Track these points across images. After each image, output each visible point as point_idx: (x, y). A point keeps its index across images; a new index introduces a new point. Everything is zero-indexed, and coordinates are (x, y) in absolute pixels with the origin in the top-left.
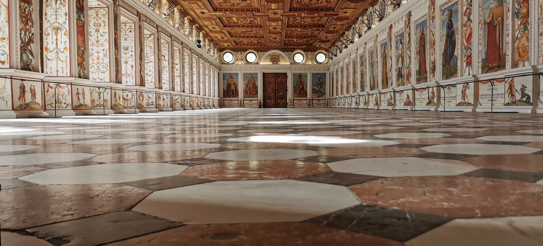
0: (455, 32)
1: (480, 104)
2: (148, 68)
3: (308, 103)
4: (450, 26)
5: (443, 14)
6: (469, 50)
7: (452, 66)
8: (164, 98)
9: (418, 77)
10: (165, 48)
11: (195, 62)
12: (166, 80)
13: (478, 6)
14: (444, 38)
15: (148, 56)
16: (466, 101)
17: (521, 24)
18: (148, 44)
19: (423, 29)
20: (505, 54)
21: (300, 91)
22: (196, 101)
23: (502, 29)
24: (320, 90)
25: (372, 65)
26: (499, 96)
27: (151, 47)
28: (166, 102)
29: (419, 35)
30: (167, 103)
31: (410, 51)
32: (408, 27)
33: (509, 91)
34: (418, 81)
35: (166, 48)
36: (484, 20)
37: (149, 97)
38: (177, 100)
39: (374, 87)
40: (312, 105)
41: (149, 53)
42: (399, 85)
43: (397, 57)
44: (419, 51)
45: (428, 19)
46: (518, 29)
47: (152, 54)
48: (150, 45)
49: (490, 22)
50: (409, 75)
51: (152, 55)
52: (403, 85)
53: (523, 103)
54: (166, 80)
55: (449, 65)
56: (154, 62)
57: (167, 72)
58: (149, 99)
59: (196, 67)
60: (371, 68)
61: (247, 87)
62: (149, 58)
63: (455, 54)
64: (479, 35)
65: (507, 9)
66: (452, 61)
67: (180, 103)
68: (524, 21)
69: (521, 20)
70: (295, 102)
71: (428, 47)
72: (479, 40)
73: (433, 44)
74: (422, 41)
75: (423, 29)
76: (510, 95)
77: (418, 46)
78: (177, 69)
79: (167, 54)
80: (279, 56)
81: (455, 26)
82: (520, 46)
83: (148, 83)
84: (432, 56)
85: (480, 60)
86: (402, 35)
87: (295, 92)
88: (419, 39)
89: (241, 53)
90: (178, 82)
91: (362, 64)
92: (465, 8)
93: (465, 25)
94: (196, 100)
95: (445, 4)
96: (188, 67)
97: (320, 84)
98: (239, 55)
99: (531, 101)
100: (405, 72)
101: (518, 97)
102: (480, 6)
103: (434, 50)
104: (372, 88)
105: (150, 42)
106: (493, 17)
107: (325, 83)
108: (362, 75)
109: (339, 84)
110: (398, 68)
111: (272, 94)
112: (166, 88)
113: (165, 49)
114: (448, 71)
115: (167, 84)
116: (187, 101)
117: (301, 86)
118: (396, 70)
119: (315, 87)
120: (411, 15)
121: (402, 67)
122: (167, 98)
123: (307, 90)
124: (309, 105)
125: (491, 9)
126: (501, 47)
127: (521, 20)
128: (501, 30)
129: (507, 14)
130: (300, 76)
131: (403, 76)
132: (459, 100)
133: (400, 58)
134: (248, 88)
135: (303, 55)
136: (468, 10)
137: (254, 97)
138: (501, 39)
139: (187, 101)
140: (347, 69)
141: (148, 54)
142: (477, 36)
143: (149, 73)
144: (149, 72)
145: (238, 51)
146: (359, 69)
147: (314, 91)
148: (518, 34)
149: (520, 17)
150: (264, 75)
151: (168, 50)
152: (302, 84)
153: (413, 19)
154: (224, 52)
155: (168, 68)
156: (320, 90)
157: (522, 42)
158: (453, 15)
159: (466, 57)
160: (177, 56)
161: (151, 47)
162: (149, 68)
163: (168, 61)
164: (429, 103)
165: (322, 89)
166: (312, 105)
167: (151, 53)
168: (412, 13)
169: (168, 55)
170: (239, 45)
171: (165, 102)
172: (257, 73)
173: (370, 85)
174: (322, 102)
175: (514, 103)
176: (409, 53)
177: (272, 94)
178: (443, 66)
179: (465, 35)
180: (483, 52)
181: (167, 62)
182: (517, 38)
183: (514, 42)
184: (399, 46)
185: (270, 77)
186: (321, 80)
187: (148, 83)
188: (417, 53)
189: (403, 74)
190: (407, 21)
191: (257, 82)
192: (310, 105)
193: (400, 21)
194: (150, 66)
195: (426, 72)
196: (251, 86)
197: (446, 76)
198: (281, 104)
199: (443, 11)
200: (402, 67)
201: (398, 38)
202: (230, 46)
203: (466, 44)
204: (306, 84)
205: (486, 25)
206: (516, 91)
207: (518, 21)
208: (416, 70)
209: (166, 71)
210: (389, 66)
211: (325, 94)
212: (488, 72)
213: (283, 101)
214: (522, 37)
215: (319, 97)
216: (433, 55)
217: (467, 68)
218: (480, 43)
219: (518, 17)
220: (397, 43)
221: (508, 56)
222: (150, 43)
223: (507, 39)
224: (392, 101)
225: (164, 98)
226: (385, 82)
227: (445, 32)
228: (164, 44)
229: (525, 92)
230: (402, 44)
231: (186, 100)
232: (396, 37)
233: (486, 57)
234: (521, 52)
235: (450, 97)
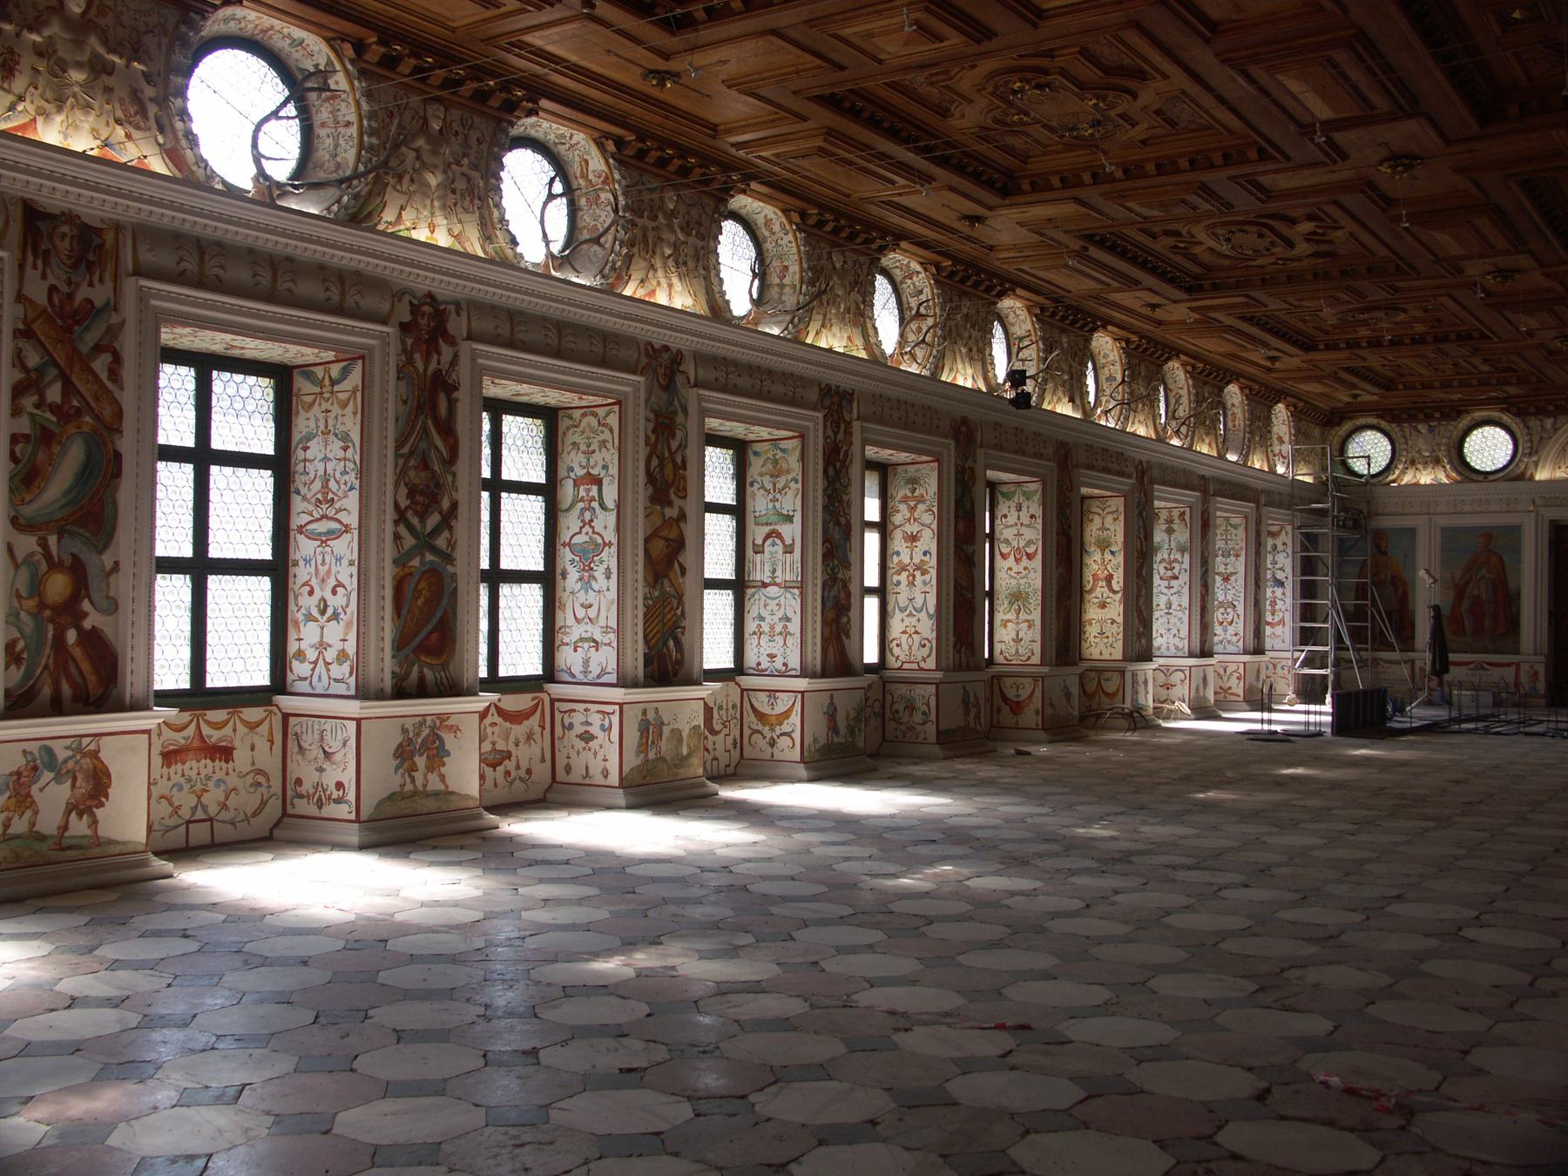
2: (329, 571)
8: (589, 728)
10: (607, 435)
11: (1036, 491)
12: (602, 622)
15: (330, 496)
18: (336, 418)
22: (1034, 700)
27: (345, 438)
28: (600, 756)
30: (605, 760)
35: (611, 430)
37: (325, 752)
38: (781, 724)
41: (338, 475)
47: (352, 478)
48: (342, 428)
51: (352, 488)
54: (602, 622)
56: (356, 533)
57: (608, 578)
58: (326, 765)
59: (1040, 521)
61: (1460, 593)
62: (337, 506)
67: (797, 736)
78: (788, 542)
79: (614, 470)
83: (327, 664)
89: (1431, 430)
90: (788, 620)
94: (1038, 694)
96: (934, 526)
98: (1421, 442)
105: (344, 405)
112: (603, 673)
113: (601, 437)
115: (609, 644)
116: (924, 713)
122: (602, 728)
134: (1466, 604)
137: (1497, 651)
139: (925, 708)
141: (332, 485)
143: (331, 600)
144: (334, 592)
145: (1419, 421)
151: (617, 444)
154: (1348, 426)
155: (614, 549)
160: (788, 472)
161: (345, 438)
162: (334, 569)
163: (618, 507)
167: (345, 472)
169: (616, 476)
170: (1401, 387)
171: (595, 754)
172: (1514, 532)
181: (611, 519)
187: (327, 664)
194: (339, 560)
202: (1359, 399)
209: (602, 569)
222: (345, 412)
225: (589, 728)
228: (601, 412)
231: (919, 703)
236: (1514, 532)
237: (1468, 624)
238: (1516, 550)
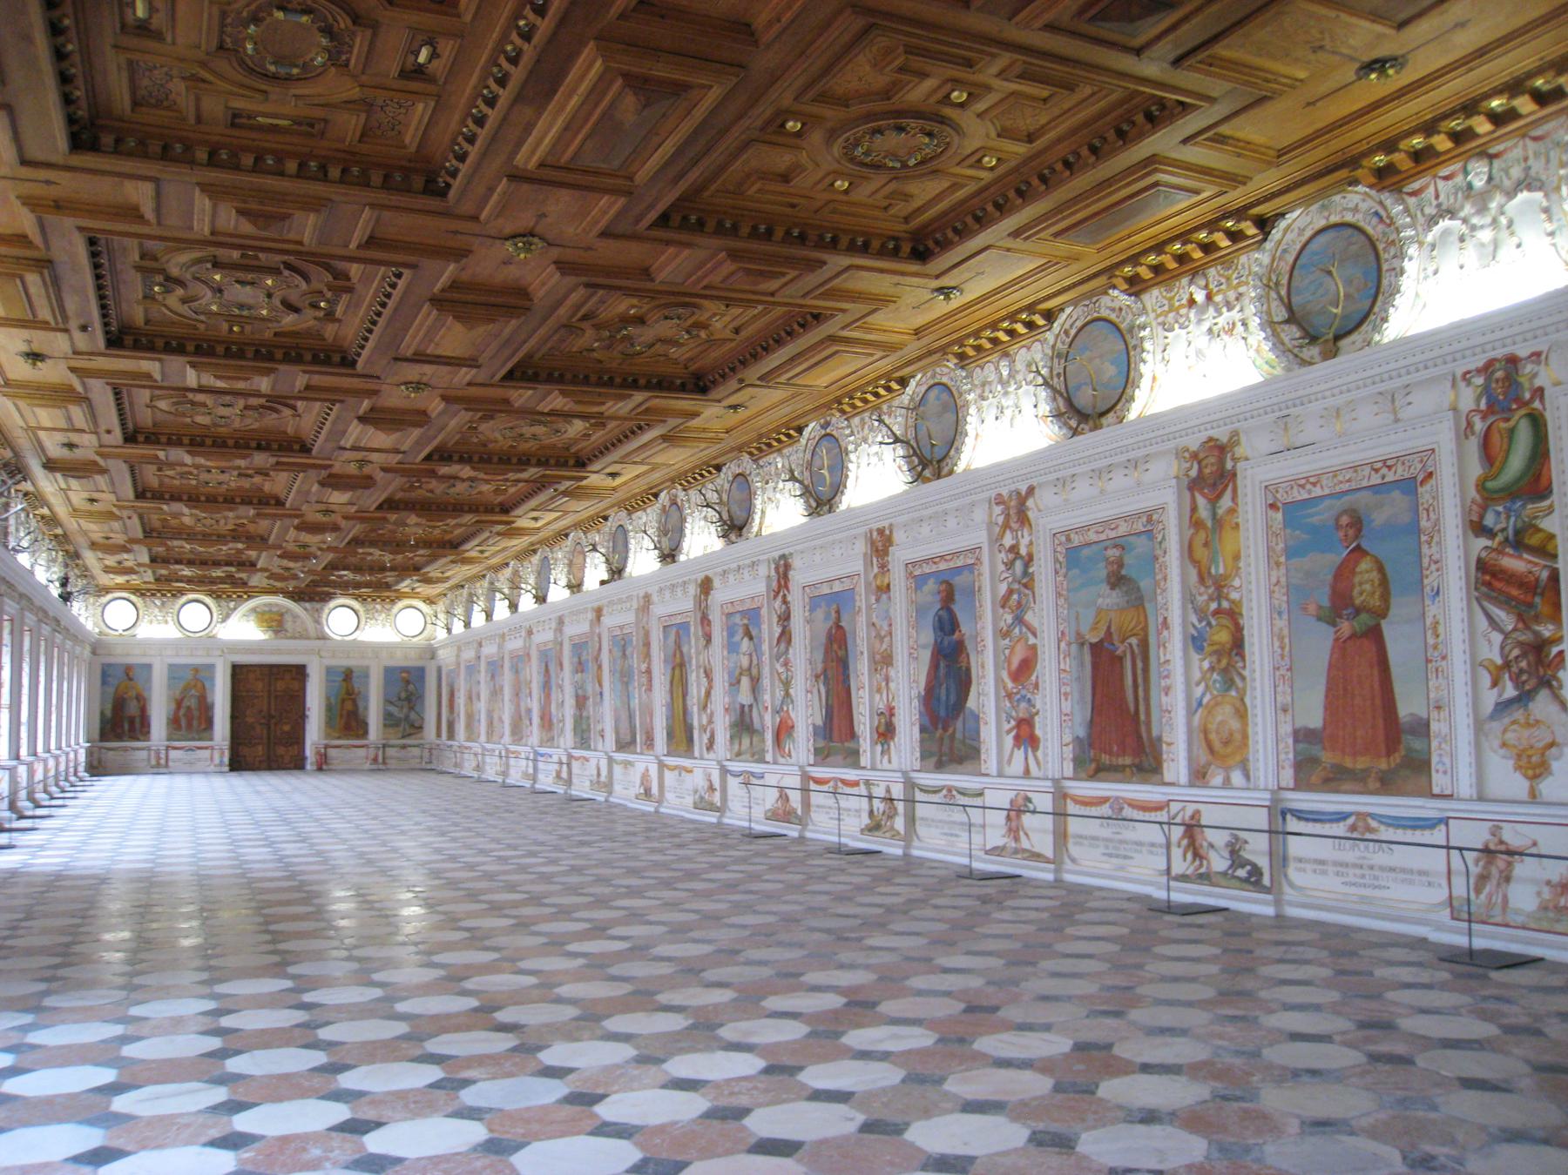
0: (969, 645)
1: (1073, 860)
3: (372, 756)
4: (947, 624)
5: (918, 588)
6: (1023, 705)
7: (959, 735)
9: (821, 744)
13: (1052, 596)
14: (926, 656)
16: (1025, 844)
17: (1212, 669)
19: (838, 612)
20: (1160, 739)
21: (347, 719)
23: (1146, 670)
24: (407, 717)
25: (623, 674)
26: (1144, 849)
29: (823, 626)
31: (786, 664)
32: (780, 598)
33: (1185, 842)
34: (822, 755)
36: (1079, 634)
39: (633, 741)
40: (384, 763)
42: (739, 754)
43: (730, 674)
44: (825, 671)
45: (861, 589)
46: (1203, 678)
49: (1101, 641)
50: (783, 731)
53: (1234, 882)
55: (945, 729)
60: (619, 686)
63: (971, 703)
64: (1061, 671)
65: (1160, 620)
66: (959, 724)
68: (1224, 662)
69: (1214, 659)
70: (332, 753)
71: (861, 669)
72: (1061, 683)
73: (887, 660)
74: (835, 646)
75: (838, 612)
76: (1189, 856)
77: (819, 656)
80: (282, 615)
81: (965, 628)
82: (1212, 727)
84: (877, 697)
85: (1068, 738)
86: (753, 615)
87: (330, 722)
88: (823, 639)
91: (580, 667)
92: (1003, 588)
93: (1006, 634)
95: (926, 561)
97: (408, 699)
99: (1266, 881)
100: (768, 721)
101: (1219, 863)
102: (1058, 595)
103: (887, 680)
104: (624, 745)
106: (1109, 633)
107: (421, 697)
108: (581, 701)
109: (482, 706)
111: (258, 728)
114: (945, 749)
117: (348, 705)
118: (726, 710)
119: (392, 709)
120: (787, 567)
121: (751, 706)
123: (366, 716)
124: (375, 760)
125: (1099, 611)
126: (1142, 717)
127: (1214, 659)
128: (1139, 672)
129: (1159, 633)
130: (348, 675)
132: (996, 837)
133: (745, 681)
135: (356, 612)
136: (1015, 596)
138: (1141, 693)
140: (516, 671)
142: (1055, 674)
146: (567, 678)
147: (390, 721)
148: (1203, 695)
149: (1208, 649)
150: (238, 671)
152: (354, 702)
153: (798, 578)
156: (407, 717)
157: (1219, 718)
158: (957, 597)
159: (1013, 723)
164: (874, 827)
165: (413, 716)
166: (384, 763)
168: (796, 562)
173: (617, 733)
174: (416, 751)
175: (1205, 878)
176: (781, 670)
177: (258, 728)
178: (923, 730)
179: (1008, 660)
180: (1078, 719)
182: (1200, 704)
183: (1190, 713)
184: (738, 644)
185: (251, 676)
186: (411, 687)
188: (817, 677)
189: (757, 724)
190: (775, 578)
191: (213, 691)
192: (380, 765)
193: (746, 575)
195: (852, 735)
196: (193, 703)
197: (934, 759)
198: (287, 759)
199: (919, 581)
200: (751, 706)
201: (737, 619)
203: (1010, 685)
204: (366, 699)
205: (1086, 649)
206: (1211, 846)
207: (1202, 660)
210: (695, 691)
211: (421, 728)
212: (1100, 775)
213: (294, 750)
214: (1217, 704)
215: (403, 737)
216: (879, 690)
217: (1019, 755)
218: (1066, 694)
219: (1199, 649)
220: (731, 632)
221: (1169, 744)
223: (1164, 699)
224: (717, 798)
226: (680, 733)
227: (928, 636)
229: (1242, 853)
230: (751, 638)
232: (729, 615)
233: (1090, 736)
234: (1217, 745)
235: (954, 823)
236: (211, 667)
237: (183, 722)
238: (212, 679)
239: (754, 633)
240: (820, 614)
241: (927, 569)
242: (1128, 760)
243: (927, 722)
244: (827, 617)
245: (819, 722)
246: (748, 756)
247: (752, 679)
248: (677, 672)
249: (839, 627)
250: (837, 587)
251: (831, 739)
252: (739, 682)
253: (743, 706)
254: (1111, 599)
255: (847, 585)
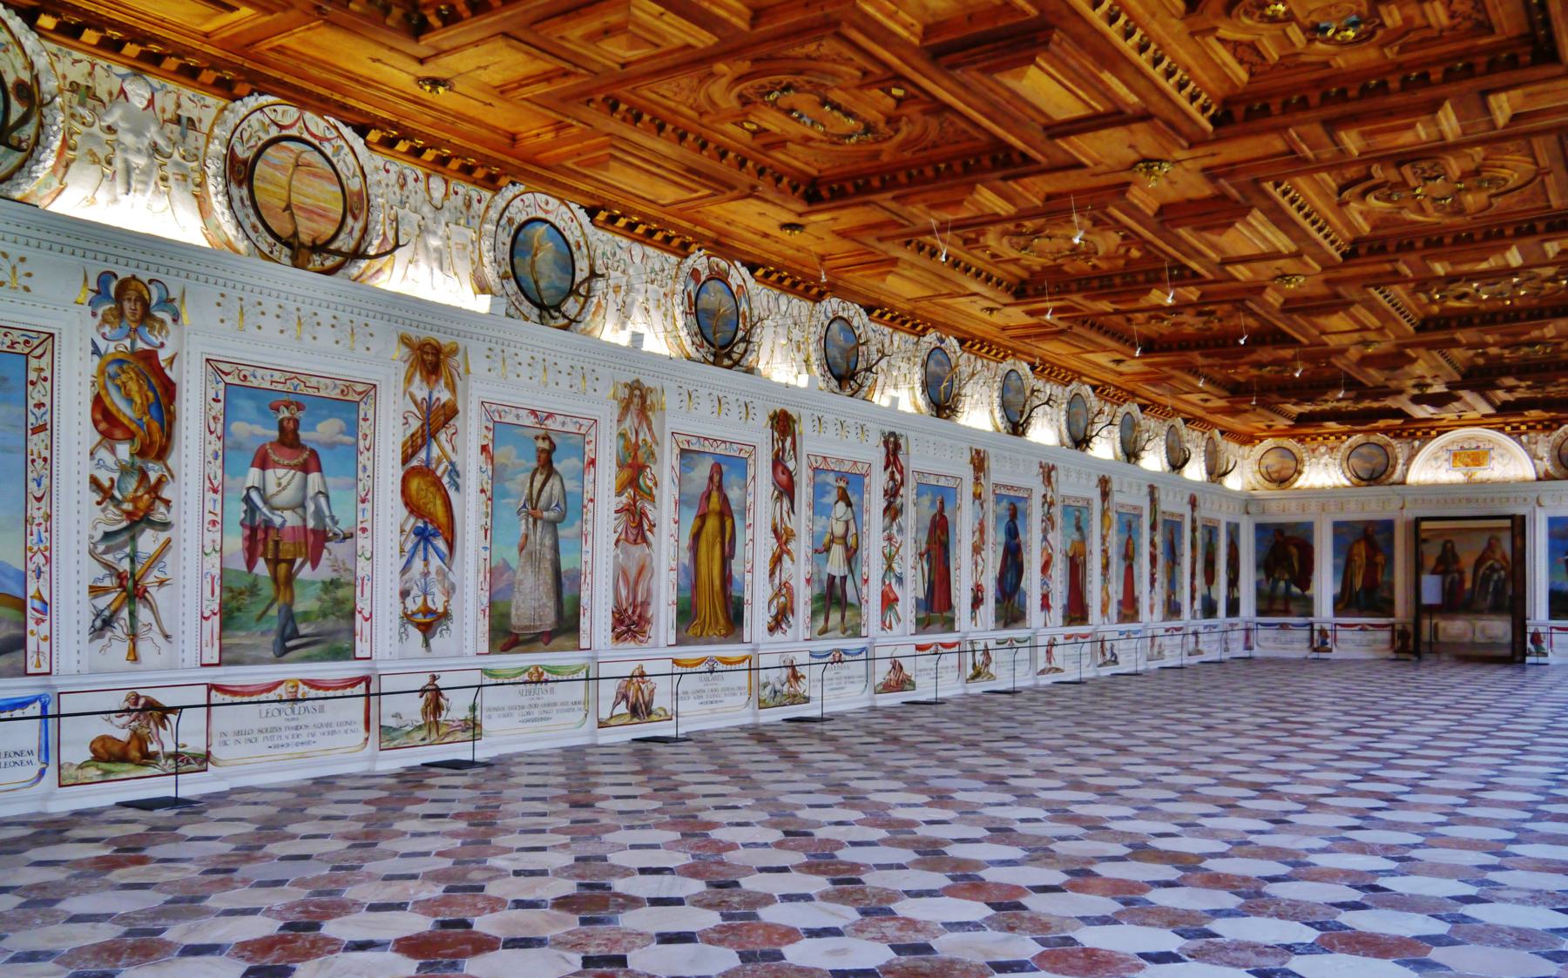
0: (1023, 547)
4: (1012, 532)
9: (922, 615)
14: (1000, 550)
19: (942, 503)
29: (928, 513)
34: (923, 625)
42: (824, 631)
44: (928, 551)
52: (850, 632)
74: (938, 532)
75: (942, 503)
77: (924, 537)
81: (1021, 536)
88: (928, 523)
95: (1005, 486)
110: (825, 578)
118: (808, 581)
121: (844, 579)
131: (852, 605)
133: (837, 551)
158: (1019, 516)
188: (921, 555)
195: (949, 606)
199: (999, 498)
200: (844, 579)
201: (831, 478)
208: (917, 599)
220: (819, 490)
227: (1002, 538)
230: (849, 504)
239: (853, 499)
240: (926, 501)
241: (1004, 492)
242: (1078, 615)
243: (1000, 596)
244: (933, 502)
245: (921, 595)
246: (838, 633)
247: (847, 548)
248: (712, 524)
249: (943, 517)
250: (942, 482)
251: (932, 611)
252: (828, 550)
253: (832, 578)
254: (1076, 536)
255: (951, 483)
